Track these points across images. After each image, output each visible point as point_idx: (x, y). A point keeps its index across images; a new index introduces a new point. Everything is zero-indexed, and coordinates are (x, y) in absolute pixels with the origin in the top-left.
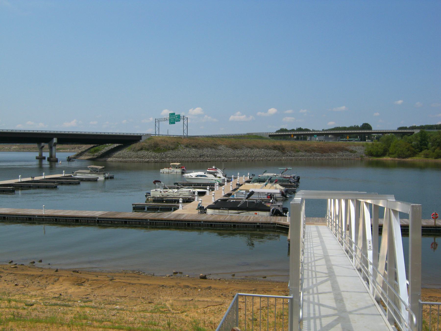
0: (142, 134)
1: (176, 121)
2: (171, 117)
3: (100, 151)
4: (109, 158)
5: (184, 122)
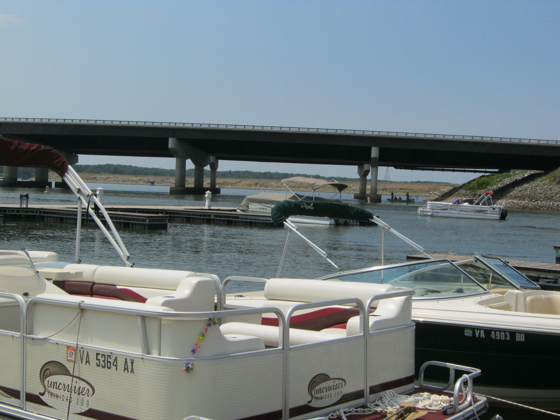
3: (491, 186)
4: (499, 199)
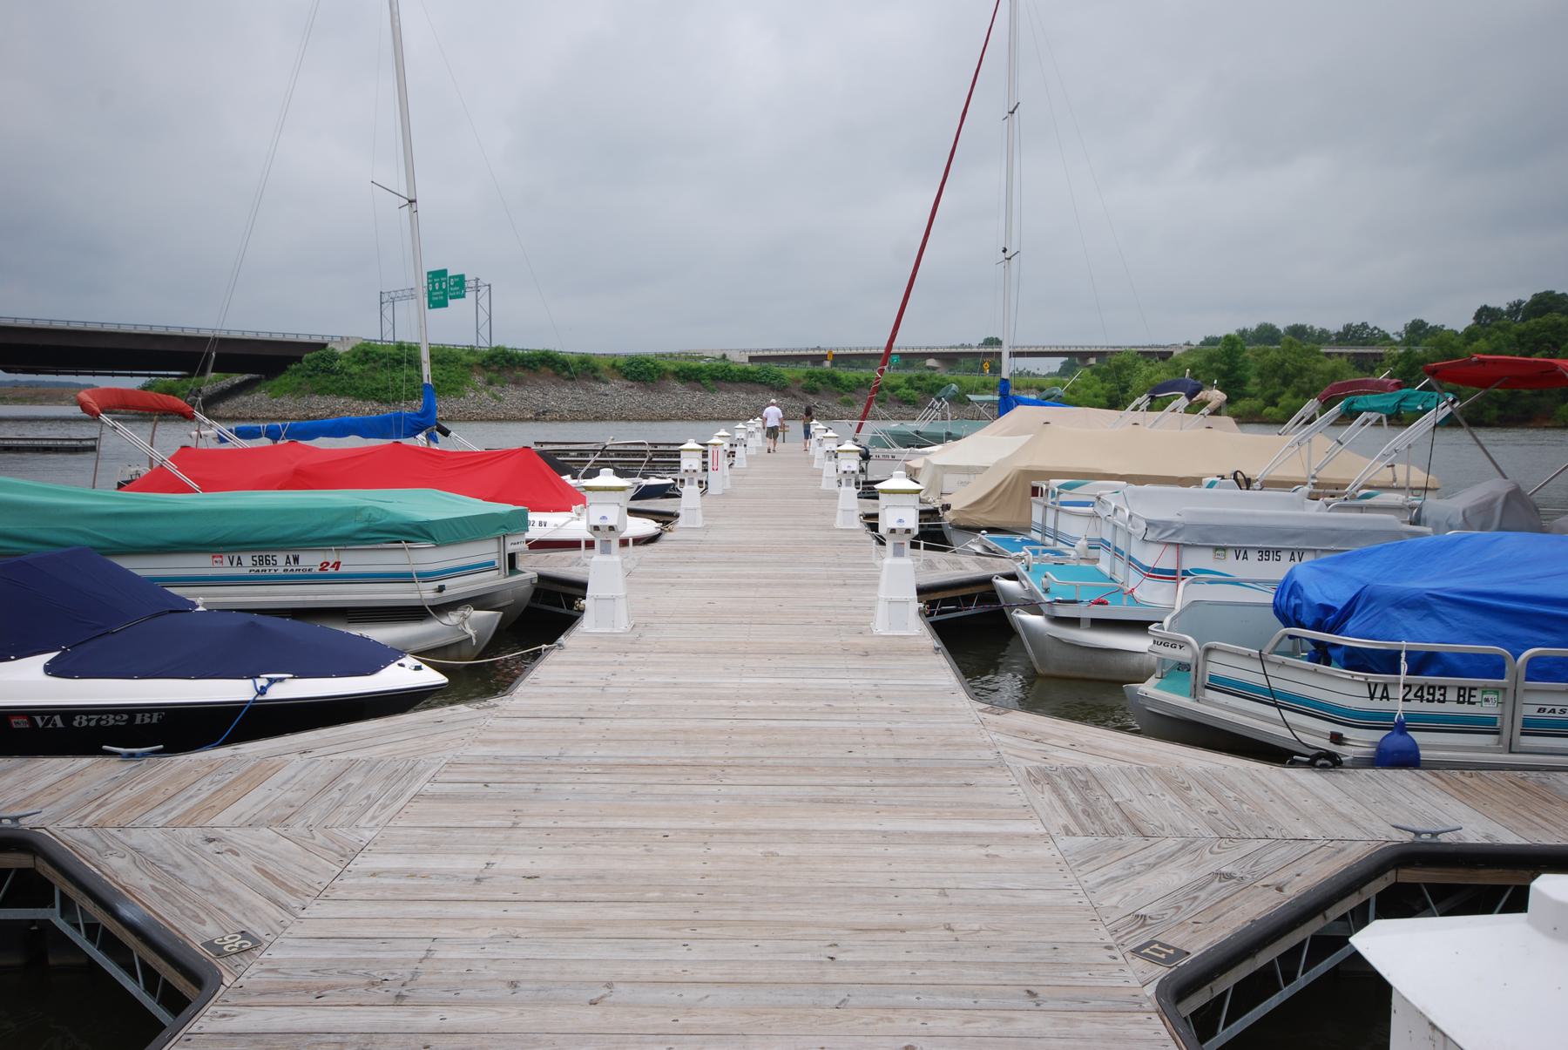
0: (326, 340)
1: (451, 298)
2: (434, 286)
5: (477, 300)
